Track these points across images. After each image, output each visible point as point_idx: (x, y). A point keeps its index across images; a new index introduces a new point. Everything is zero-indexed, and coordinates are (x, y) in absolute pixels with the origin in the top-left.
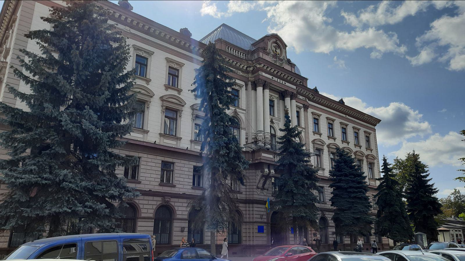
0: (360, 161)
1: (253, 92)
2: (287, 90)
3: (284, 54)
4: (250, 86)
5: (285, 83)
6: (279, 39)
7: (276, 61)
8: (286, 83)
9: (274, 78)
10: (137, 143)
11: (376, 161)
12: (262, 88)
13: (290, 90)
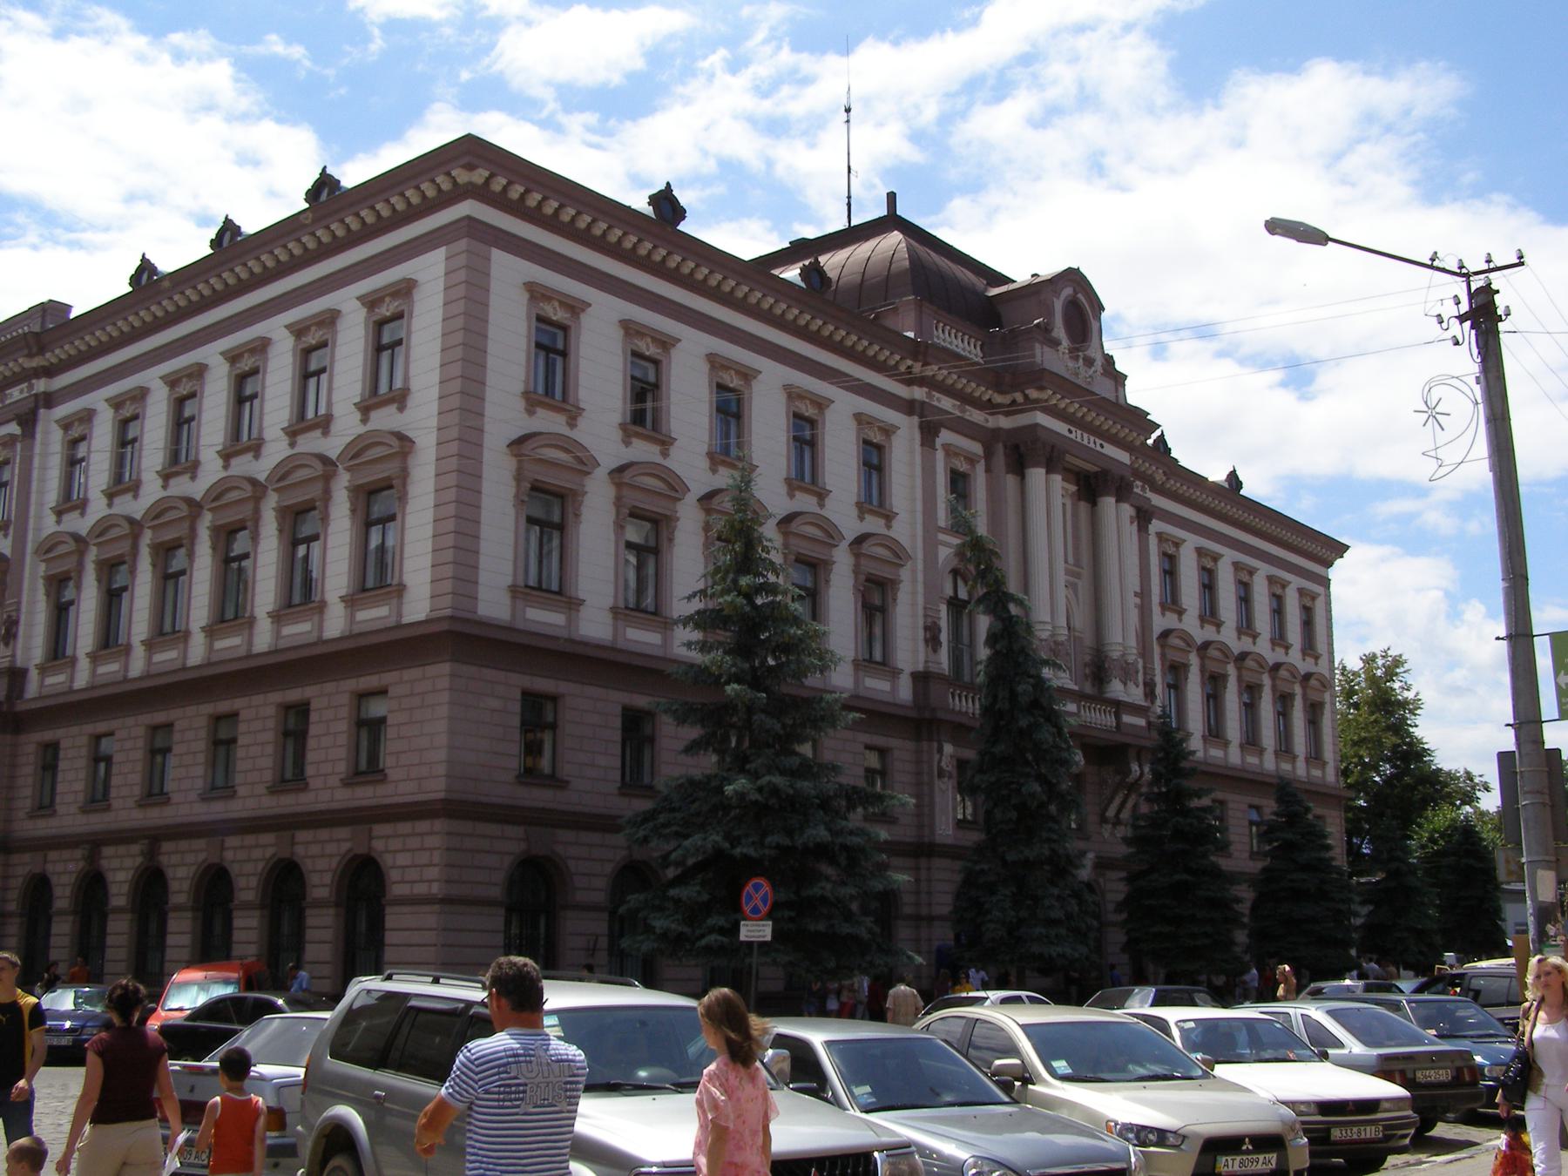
1: (1011, 481)
4: (1000, 460)
5: (1102, 446)
8: (1105, 444)
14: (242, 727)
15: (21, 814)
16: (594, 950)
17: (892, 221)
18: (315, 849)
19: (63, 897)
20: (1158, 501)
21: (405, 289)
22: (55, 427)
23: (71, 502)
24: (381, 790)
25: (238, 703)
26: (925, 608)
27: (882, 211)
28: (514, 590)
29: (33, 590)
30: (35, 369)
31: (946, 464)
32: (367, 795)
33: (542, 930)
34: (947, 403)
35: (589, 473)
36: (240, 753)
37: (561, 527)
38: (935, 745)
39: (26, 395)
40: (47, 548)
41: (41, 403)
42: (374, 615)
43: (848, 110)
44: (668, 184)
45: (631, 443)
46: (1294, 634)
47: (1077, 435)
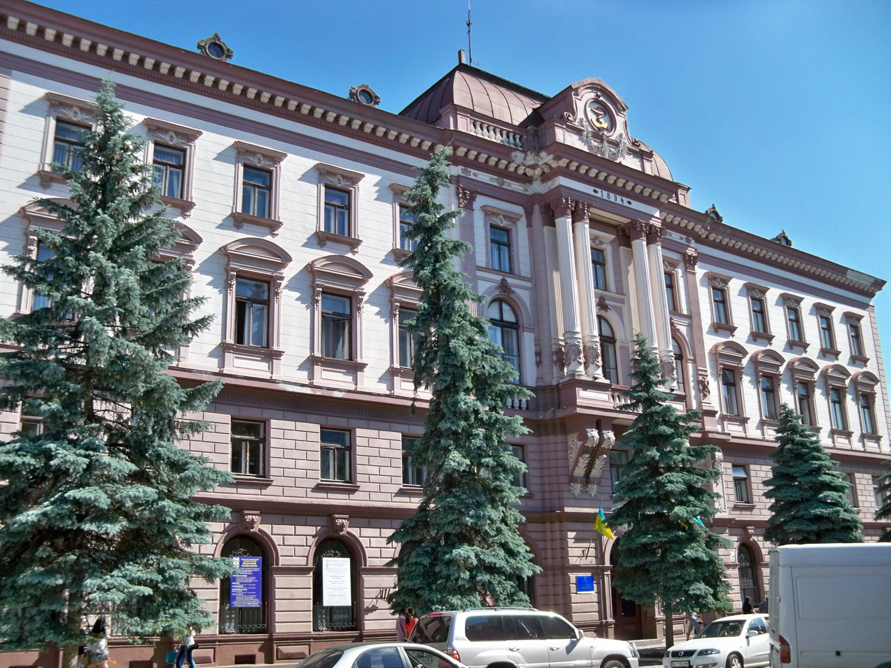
8: (631, 201)
9: (599, 190)
11: (877, 388)
34: (484, 177)
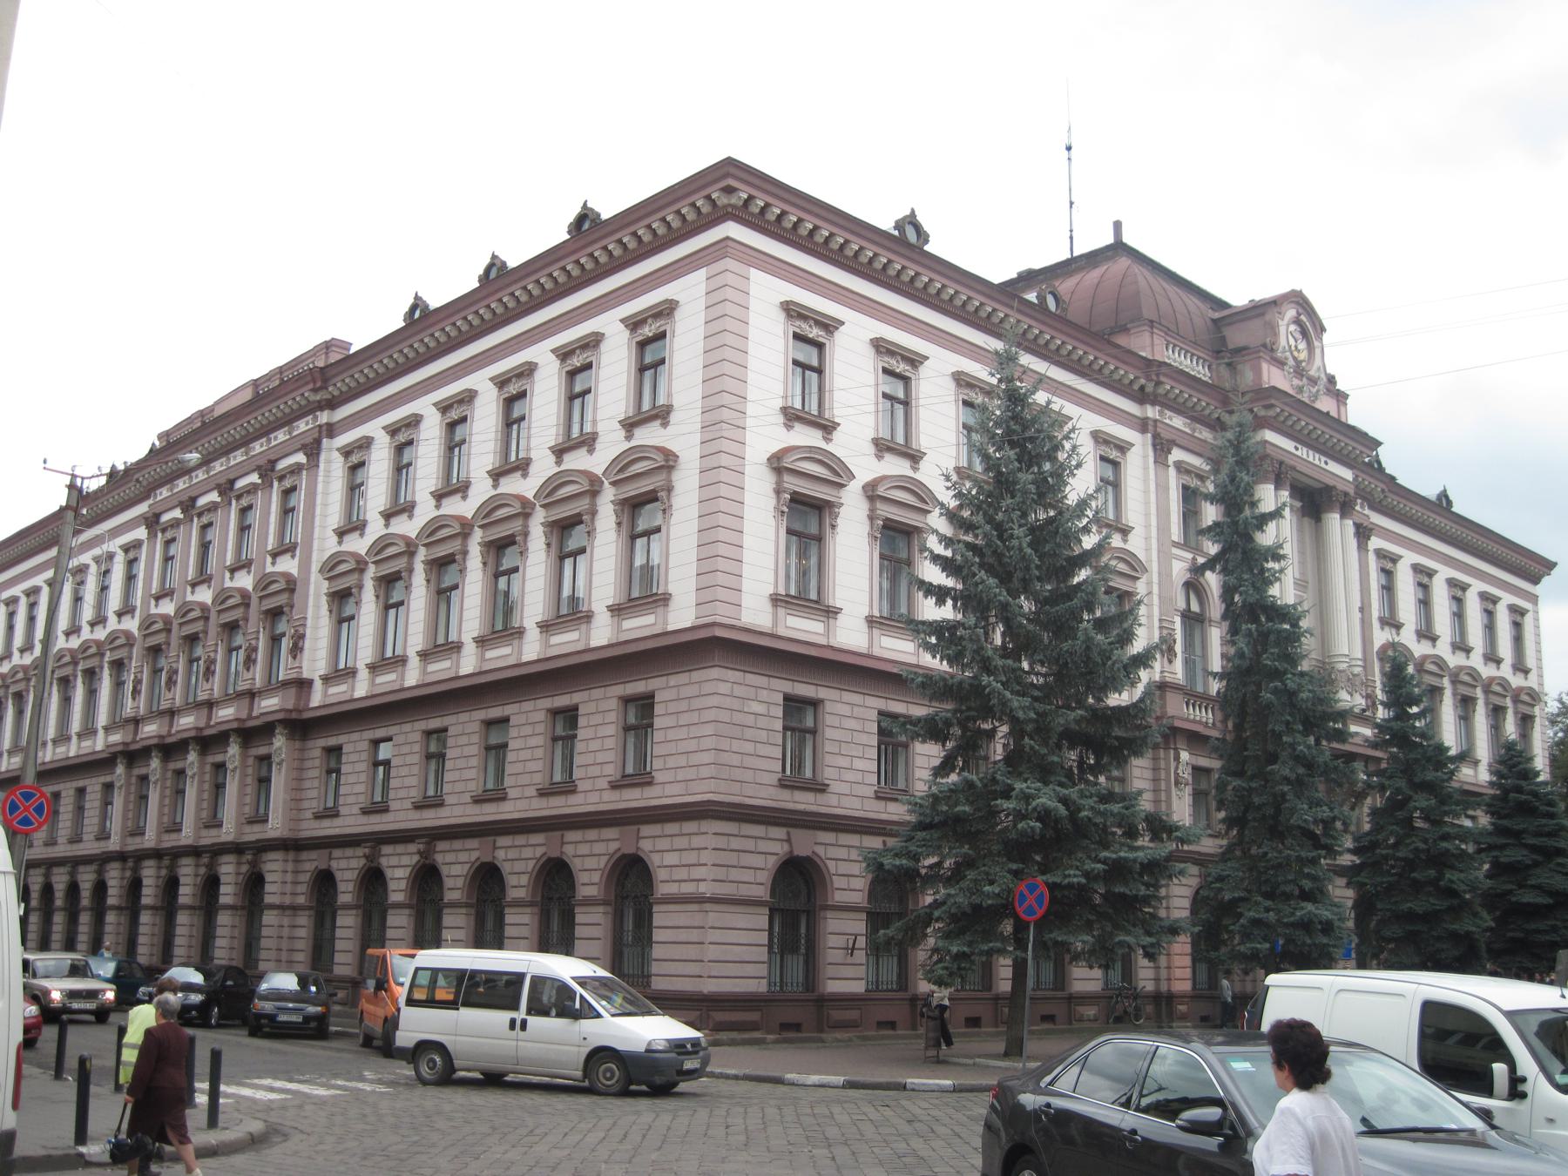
0: (1435, 691)
2: (1334, 487)
3: (1318, 362)
6: (1303, 308)
7: (1300, 389)
10: (813, 652)
12: (1272, 487)
13: (1340, 486)
14: (513, 732)
15: (309, 814)
16: (853, 948)
17: (1119, 248)
18: (584, 849)
19: (346, 892)
20: (1377, 519)
21: (666, 310)
22: (338, 459)
23: (352, 526)
24: (649, 792)
25: (508, 710)
26: (1160, 620)
27: (1109, 239)
28: (776, 600)
29: (317, 607)
30: (319, 402)
31: (1178, 479)
32: (634, 798)
33: (803, 930)
34: (1178, 422)
35: (845, 486)
36: (510, 757)
37: (819, 539)
38: (1172, 752)
39: (310, 426)
40: (331, 567)
41: (324, 433)
42: (640, 625)
43: (1069, 148)
44: (913, 211)
45: (883, 457)
46: (1505, 649)
47: (1303, 452)
